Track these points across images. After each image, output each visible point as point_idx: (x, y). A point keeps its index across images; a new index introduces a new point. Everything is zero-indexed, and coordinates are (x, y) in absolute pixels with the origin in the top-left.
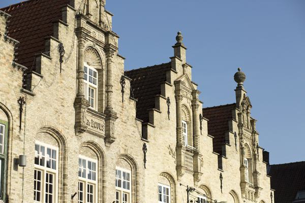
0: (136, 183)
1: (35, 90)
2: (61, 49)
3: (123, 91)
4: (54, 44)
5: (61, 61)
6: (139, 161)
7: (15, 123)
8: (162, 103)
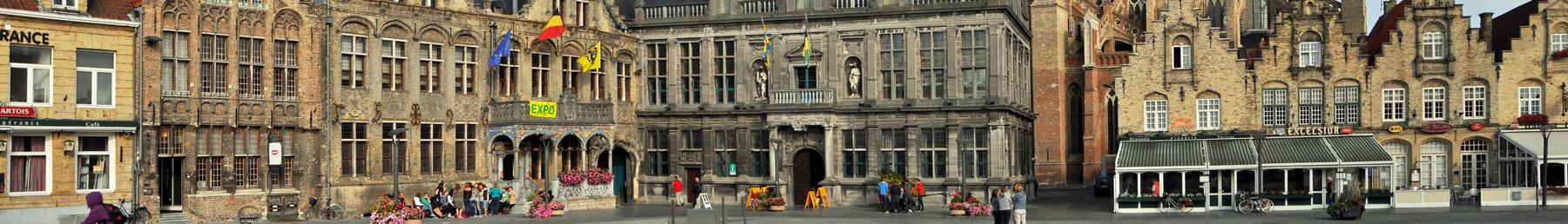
0: (1488, 93)
1: (1377, 64)
2: (1400, 34)
3: (1469, 39)
4: (1394, 35)
5: (1400, 41)
6: (1491, 79)
8: (1524, 31)
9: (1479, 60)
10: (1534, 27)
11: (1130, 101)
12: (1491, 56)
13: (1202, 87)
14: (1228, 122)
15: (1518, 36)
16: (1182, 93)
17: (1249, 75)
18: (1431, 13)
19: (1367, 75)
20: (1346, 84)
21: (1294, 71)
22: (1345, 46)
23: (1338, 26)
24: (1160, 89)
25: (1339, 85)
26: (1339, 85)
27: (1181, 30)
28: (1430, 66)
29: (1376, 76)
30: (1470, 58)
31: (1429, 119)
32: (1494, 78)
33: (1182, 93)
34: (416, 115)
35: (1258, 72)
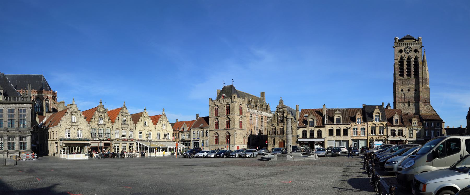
2: (118, 118)
7: (111, 129)
8: (140, 120)
9: (132, 125)
10: (141, 119)
11: (62, 130)
12: (134, 124)
14: (84, 136)
15: (138, 121)
16: (74, 129)
17: (89, 125)
18: (124, 114)
19: (112, 126)
20: (108, 128)
21: (99, 125)
22: (108, 120)
23: (107, 115)
24: (69, 127)
25: (107, 129)
26: (107, 129)
27: (74, 113)
29: (114, 127)
31: (123, 138)
32: (135, 129)
33: (74, 129)
35: (91, 124)
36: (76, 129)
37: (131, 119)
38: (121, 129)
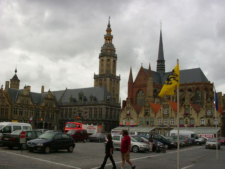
13: (131, 118)
20: (152, 118)
28: (165, 115)
29: (157, 117)
30: (172, 114)
34: (23, 118)
36: (129, 119)
37: (171, 109)
38: (163, 118)
